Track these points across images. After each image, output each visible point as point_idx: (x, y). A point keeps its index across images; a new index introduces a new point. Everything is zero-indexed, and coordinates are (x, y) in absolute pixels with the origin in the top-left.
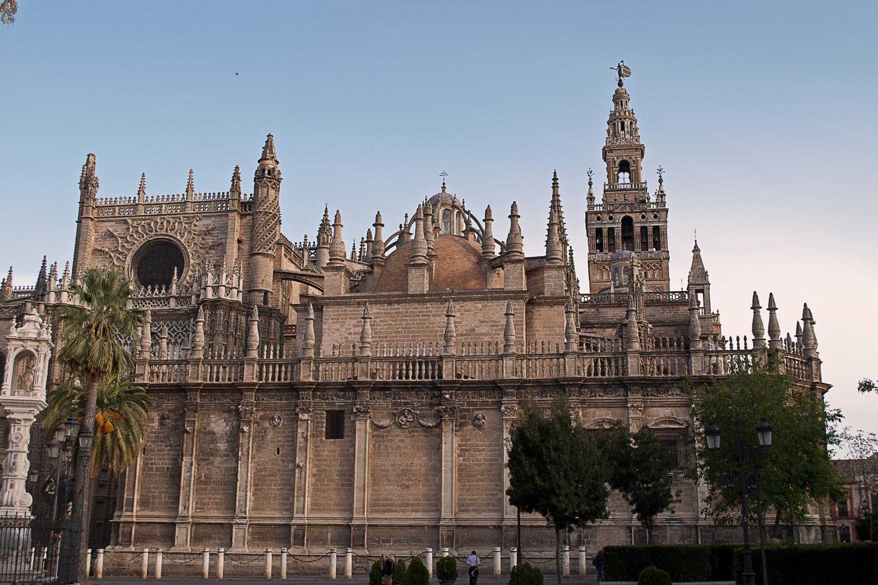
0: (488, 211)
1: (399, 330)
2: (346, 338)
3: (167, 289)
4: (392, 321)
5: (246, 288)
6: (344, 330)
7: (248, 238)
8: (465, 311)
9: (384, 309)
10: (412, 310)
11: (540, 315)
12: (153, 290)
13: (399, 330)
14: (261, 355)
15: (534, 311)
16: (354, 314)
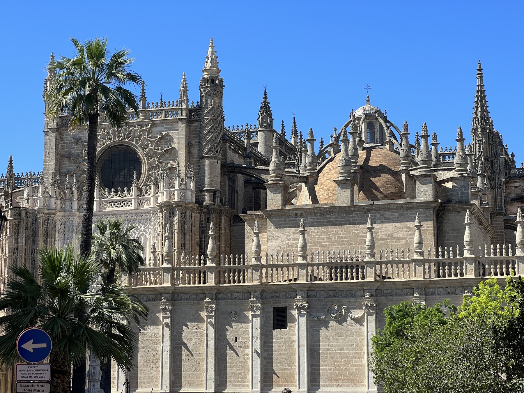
0: (406, 127)
1: (331, 236)
2: (287, 244)
3: (129, 190)
4: (324, 229)
5: (197, 188)
6: (285, 237)
7: (197, 142)
8: (385, 219)
9: (317, 219)
10: (340, 219)
11: (449, 220)
12: (116, 192)
13: (331, 236)
14: (218, 260)
15: (443, 216)
16: (292, 224)
